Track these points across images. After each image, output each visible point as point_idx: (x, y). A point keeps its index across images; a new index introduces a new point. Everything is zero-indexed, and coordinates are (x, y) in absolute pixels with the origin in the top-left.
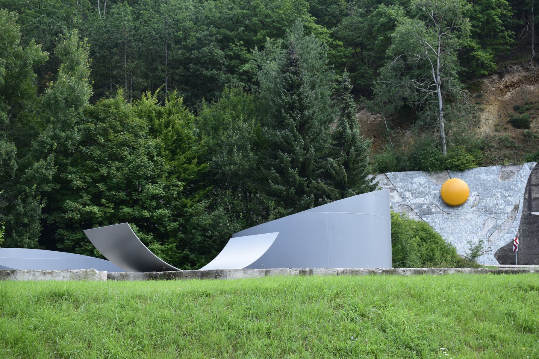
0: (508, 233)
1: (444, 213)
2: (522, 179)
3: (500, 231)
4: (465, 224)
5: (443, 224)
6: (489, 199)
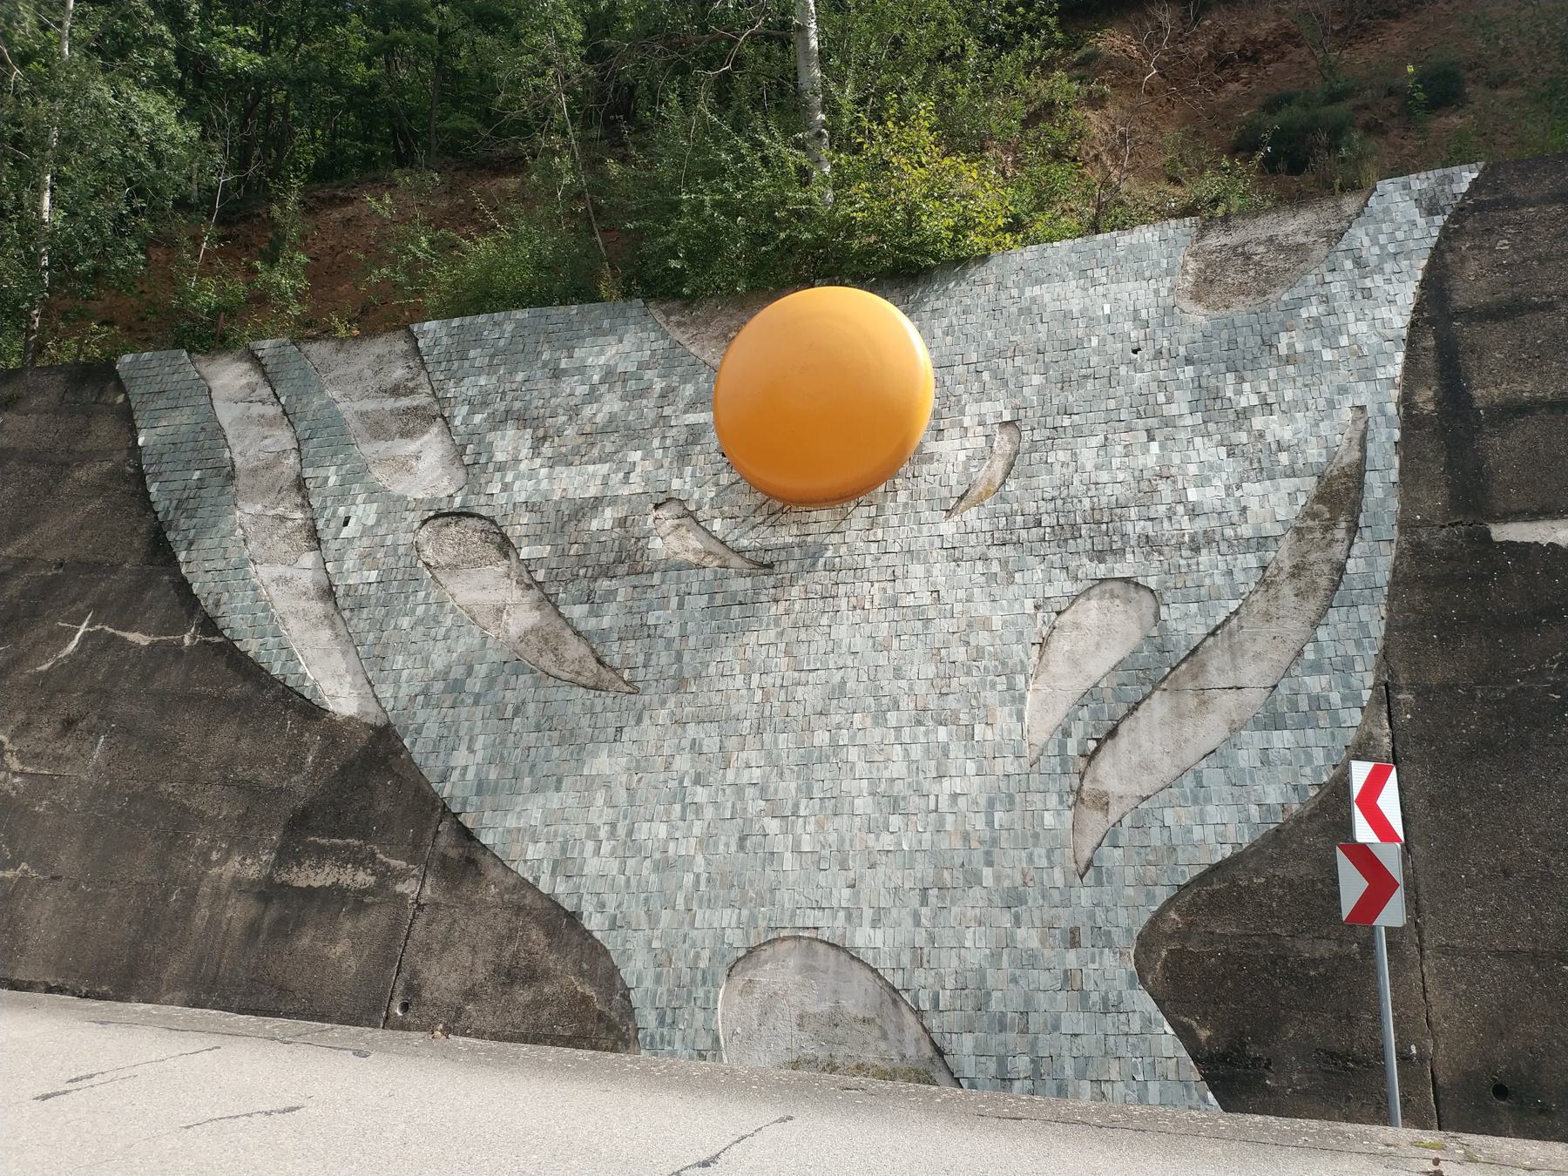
0: (1274, 722)
1: (736, 561)
2: (1368, 283)
3: (1190, 701)
4: (881, 647)
5: (711, 645)
6: (1095, 441)
